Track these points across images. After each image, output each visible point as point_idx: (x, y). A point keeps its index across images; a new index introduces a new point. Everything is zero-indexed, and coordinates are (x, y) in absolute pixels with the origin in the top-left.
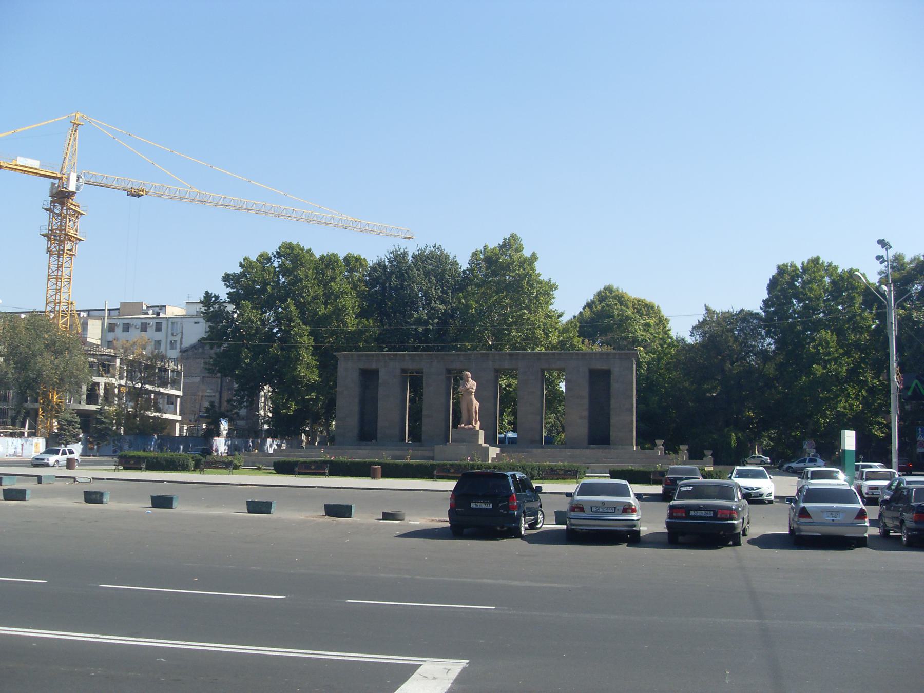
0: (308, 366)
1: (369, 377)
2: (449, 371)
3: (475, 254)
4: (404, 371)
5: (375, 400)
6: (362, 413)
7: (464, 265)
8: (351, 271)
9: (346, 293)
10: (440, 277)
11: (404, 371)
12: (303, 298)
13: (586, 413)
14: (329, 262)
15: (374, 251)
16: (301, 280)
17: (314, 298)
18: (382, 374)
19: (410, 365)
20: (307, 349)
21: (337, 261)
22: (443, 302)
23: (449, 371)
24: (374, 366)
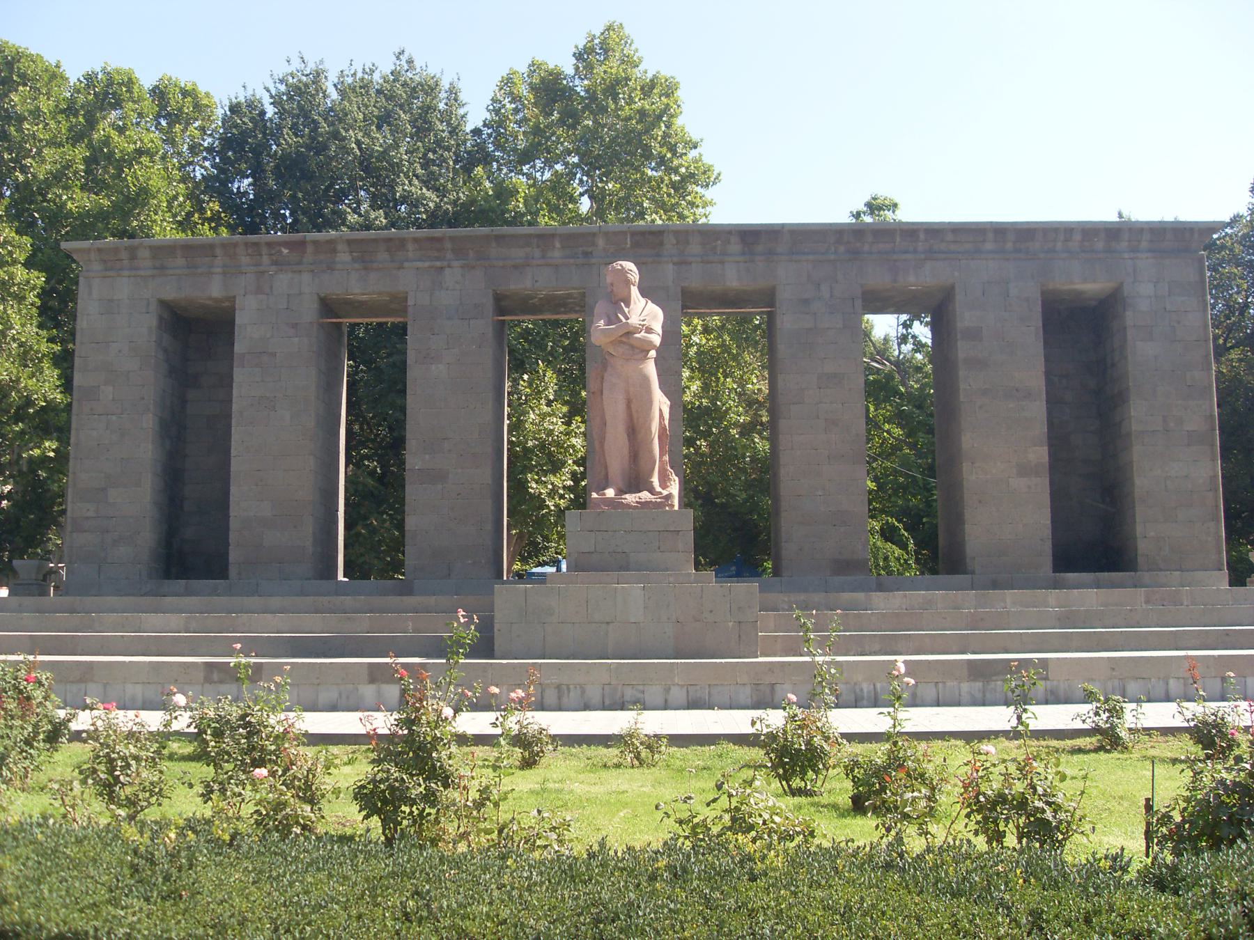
1: (196, 338)
2: (503, 305)
3: (508, 82)
4: (328, 307)
6: (173, 476)
7: (475, 115)
8: (174, 118)
10: (422, 126)
11: (328, 307)
12: (24, 169)
13: (1040, 454)
14: (108, 92)
15: (235, 71)
16: (21, 119)
17: (58, 178)
19: (355, 285)
20: (20, 299)
21: (130, 83)
22: (429, 181)
23: (503, 305)
24: (216, 290)
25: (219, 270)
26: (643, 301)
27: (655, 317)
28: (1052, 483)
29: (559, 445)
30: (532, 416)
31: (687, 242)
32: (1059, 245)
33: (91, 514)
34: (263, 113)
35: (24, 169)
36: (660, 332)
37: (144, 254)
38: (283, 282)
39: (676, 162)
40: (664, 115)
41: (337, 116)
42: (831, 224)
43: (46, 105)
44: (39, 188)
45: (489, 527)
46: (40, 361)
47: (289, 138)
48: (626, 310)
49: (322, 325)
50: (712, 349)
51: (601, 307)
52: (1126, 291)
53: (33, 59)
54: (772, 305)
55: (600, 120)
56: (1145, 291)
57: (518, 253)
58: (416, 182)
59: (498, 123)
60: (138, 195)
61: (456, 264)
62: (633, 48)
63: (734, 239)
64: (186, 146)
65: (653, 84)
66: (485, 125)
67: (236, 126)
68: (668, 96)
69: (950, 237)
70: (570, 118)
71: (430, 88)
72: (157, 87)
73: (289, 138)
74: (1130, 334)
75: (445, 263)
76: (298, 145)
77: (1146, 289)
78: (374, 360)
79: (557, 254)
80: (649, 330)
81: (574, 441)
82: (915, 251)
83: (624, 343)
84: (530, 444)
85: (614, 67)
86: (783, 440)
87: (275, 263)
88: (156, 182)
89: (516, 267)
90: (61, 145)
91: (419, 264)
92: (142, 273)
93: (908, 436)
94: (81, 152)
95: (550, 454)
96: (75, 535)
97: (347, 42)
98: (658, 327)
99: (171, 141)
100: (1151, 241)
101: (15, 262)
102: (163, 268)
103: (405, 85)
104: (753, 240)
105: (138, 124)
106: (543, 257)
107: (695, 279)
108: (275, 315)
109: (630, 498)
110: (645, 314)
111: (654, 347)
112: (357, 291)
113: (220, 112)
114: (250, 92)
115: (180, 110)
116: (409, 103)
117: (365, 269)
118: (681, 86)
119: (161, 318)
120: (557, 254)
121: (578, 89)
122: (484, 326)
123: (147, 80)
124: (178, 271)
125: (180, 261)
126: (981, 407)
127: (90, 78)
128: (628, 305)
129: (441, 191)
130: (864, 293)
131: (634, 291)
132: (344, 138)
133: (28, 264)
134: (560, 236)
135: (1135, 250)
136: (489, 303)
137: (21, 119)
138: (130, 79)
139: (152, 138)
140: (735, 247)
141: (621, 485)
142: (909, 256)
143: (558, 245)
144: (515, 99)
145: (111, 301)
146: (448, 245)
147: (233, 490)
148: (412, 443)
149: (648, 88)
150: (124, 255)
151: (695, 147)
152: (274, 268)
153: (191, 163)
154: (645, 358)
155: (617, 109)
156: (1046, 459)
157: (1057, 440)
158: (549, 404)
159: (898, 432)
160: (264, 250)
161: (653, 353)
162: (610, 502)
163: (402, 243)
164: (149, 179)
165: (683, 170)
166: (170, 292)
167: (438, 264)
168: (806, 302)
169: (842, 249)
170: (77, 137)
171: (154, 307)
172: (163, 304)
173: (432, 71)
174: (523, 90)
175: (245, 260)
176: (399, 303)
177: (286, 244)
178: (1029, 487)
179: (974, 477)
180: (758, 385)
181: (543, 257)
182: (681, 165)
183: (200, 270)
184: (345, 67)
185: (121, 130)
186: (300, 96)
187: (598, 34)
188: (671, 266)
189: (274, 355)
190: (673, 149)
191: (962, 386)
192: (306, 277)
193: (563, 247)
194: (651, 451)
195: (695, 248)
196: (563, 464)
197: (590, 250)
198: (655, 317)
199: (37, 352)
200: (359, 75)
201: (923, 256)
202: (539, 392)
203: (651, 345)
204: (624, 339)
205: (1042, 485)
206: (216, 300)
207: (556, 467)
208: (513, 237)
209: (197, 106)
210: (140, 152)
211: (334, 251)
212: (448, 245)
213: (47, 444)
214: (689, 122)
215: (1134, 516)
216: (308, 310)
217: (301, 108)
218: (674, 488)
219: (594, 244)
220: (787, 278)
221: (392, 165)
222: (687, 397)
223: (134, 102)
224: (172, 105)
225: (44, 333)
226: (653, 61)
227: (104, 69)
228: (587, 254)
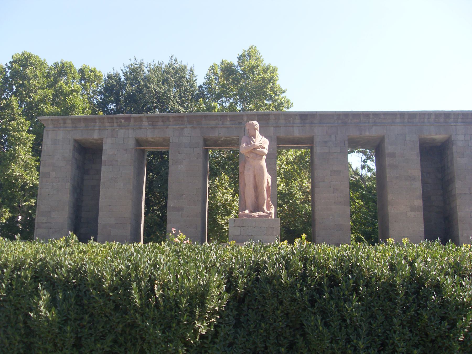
0: (26, 167)
1: (88, 155)
2: (208, 143)
3: (212, 68)
4: (139, 143)
5: (96, 189)
7: (200, 80)
8: (87, 80)
9: (77, 92)
10: (179, 84)
11: (139, 143)
12: (30, 97)
13: (419, 202)
14: (62, 70)
15: (110, 62)
16: (29, 79)
17: (43, 101)
18: (106, 147)
19: (149, 134)
20: (25, 144)
21: (70, 67)
22: (182, 104)
23: (208, 143)
24: (96, 136)
25: (97, 128)
26: (261, 137)
27: (265, 143)
28: (424, 215)
29: (230, 205)
30: (219, 193)
31: (279, 119)
32: (426, 120)
33: (44, 221)
34: (120, 79)
35: (30, 97)
36: (268, 149)
37: (69, 121)
38: (121, 133)
39: (276, 98)
40: (271, 80)
41: (147, 79)
42: (335, 112)
43: (39, 74)
44: (35, 105)
45: (200, 229)
46: (31, 168)
47: (129, 87)
48: (254, 140)
49: (136, 150)
50: (290, 170)
51: (244, 139)
52: (453, 138)
53: (35, 57)
54: (312, 143)
55: (247, 83)
56: (460, 138)
57: (213, 123)
58: (176, 104)
59: (208, 83)
60: (71, 107)
61: (189, 126)
62: (261, 55)
63: (297, 118)
64: (91, 91)
65: (268, 68)
66: (204, 84)
67: (110, 83)
68: (273, 73)
69: (382, 117)
70: (236, 82)
71: (183, 69)
72: (81, 69)
73: (129, 87)
74: (455, 155)
75: (185, 126)
76: (133, 90)
77: (461, 137)
78: (156, 165)
79: (228, 123)
80: (263, 148)
81: (235, 203)
82: (369, 122)
83: (253, 152)
84: (218, 204)
85: (252, 62)
86: (316, 196)
87: (119, 126)
88: (78, 103)
89: (212, 128)
90: (44, 89)
91: (174, 127)
92: (68, 129)
93: (365, 204)
94: (51, 91)
95: (226, 208)
96: (38, 229)
97: (152, 54)
98: (267, 146)
99: (85, 89)
100: (462, 118)
101: (24, 130)
102: (76, 127)
103: (173, 69)
104: (306, 118)
105: (73, 82)
106: (223, 124)
107: (282, 133)
108: (118, 147)
109: (255, 214)
110: (262, 142)
111: (265, 154)
112: (150, 137)
113: (104, 78)
114: (115, 72)
115: (89, 77)
116: (176, 76)
117: (154, 128)
118: (278, 69)
119: (74, 146)
120: (228, 123)
121: (239, 71)
122: (199, 150)
123: (77, 66)
124: (81, 128)
125: (83, 125)
126: (395, 184)
127: (56, 65)
128: (255, 138)
129: (186, 108)
130: (349, 139)
131: (257, 133)
132: (149, 87)
133: (29, 132)
134: (229, 115)
135: (456, 122)
136: (201, 142)
137: (29, 79)
138: (70, 65)
139: (77, 85)
140: (298, 121)
141: (251, 209)
142: (366, 125)
143: (228, 119)
144: (215, 74)
145: (56, 139)
146: (186, 119)
147: (100, 213)
148: (170, 196)
149: (266, 70)
150: (61, 122)
151: (284, 93)
152: (118, 127)
153: (92, 97)
154: (261, 159)
155: (253, 77)
156: (421, 204)
157: (426, 197)
158: (226, 189)
159: (362, 203)
160: (115, 121)
161: (264, 157)
162: (247, 215)
163: (168, 118)
164: (76, 101)
165: (279, 101)
166: (78, 136)
167: (182, 126)
168: (326, 142)
169: (340, 121)
170: (49, 87)
171: (72, 142)
172: (75, 141)
173: (183, 64)
174: (220, 72)
175: (107, 124)
176: (166, 142)
177: (123, 118)
178: (415, 215)
179: (393, 211)
180: (307, 185)
181: (223, 124)
182: (278, 99)
183: (90, 128)
184: (151, 62)
185: (67, 84)
186: (134, 73)
187: (247, 50)
188: (272, 128)
189: (117, 161)
190: (275, 93)
191: (388, 175)
192: (131, 131)
193: (230, 120)
194: (263, 196)
195: (282, 121)
196: (231, 212)
197: (241, 121)
198: (265, 143)
199: (31, 165)
200: (157, 65)
201: (372, 124)
202: (222, 184)
203: (264, 153)
204: (253, 151)
205: (420, 215)
206: (96, 140)
207: (229, 213)
208: (210, 116)
209: (96, 76)
210: (73, 91)
211: (142, 121)
212: (186, 119)
213: (32, 200)
214: (281, 83)
215: (458, 228)
216: (131, 144)
217: (134, 77)
218: (273, 210)
219: (242, 119)
220: (318, 133)
221: (167, 97)
222: (280, 188)
223: (72, 74)
224: (86, 76)
225: (34, 158)
226: (267, 58)
227: (61, 62)
228: (240, 123)
